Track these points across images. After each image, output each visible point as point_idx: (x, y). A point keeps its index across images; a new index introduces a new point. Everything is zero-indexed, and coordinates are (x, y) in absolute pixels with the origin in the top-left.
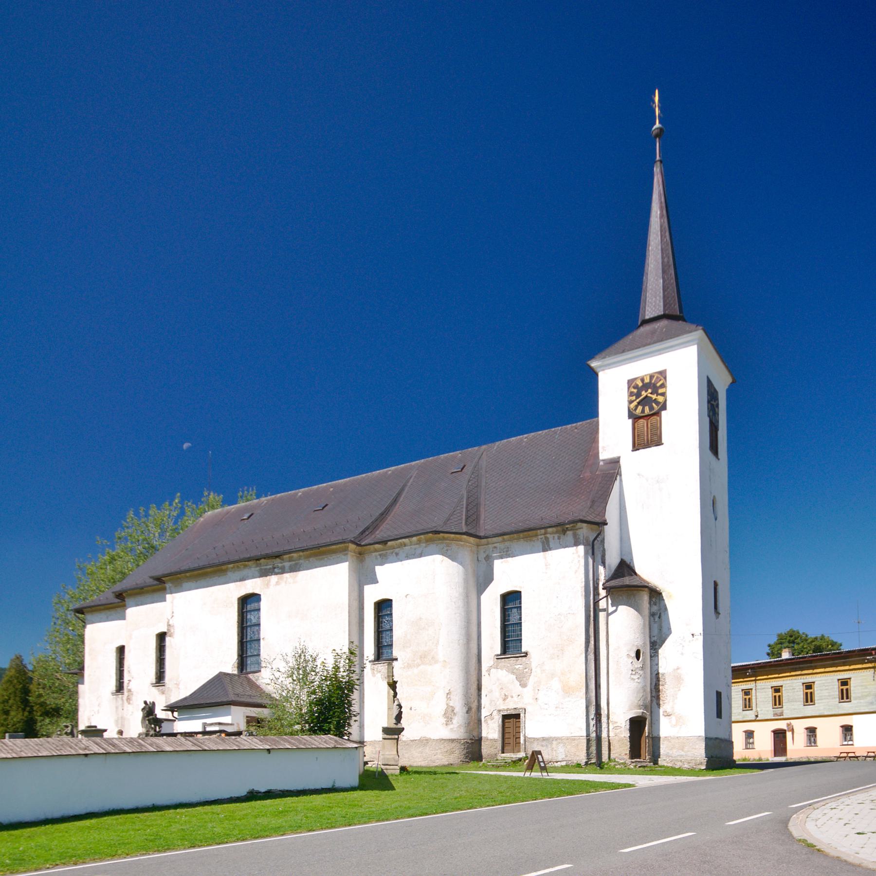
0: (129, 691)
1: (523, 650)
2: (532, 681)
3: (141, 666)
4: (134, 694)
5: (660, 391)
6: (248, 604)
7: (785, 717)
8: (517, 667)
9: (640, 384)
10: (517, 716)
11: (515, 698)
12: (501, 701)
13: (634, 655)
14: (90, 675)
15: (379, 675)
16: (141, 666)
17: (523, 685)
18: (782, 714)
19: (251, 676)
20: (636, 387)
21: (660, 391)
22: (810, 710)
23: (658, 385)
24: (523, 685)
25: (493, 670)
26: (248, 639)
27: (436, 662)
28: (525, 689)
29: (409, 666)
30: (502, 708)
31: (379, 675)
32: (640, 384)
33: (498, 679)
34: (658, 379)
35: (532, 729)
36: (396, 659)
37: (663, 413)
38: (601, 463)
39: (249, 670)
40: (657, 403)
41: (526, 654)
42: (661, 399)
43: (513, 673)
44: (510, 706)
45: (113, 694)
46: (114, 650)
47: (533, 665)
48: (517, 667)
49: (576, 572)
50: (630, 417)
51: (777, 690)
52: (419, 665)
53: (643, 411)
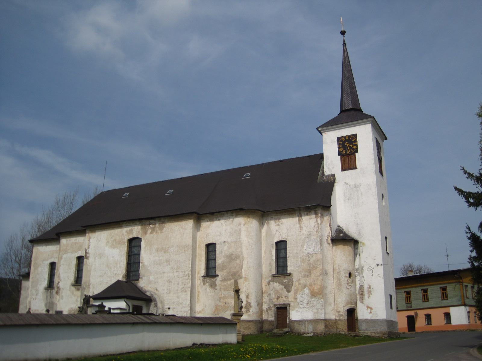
0: (58, 288)
1: (288, 272)
2: (293, 289)
3: (66, 275)
4: (61, 289)
5: (354, 144)
6: (134, 244)
7: (413, 308)
8: (285, 281)
9: (344, 140)
10: (286, 308)
11: (284, 299)
12: (276, 299)
13: (348, 275)
14: (33, 278)
15: (207, 284)
16: (66, 275)
17: (289, 291)
18: (411, 307)
19: (133, 282)
20: (342, 141)
21: (354, 144)
22: (426, 305)
23: (353, 141)
24: (289, 291)
25: (271, 283)
26: (132, 261)
28: (290, 294)
29: (225, 280)
30: (276, 303)
31: (207, 284)
32: (344, 140)
33: (274, 288)
34: (353, 138)
35: (294, 315)
37: (356, 154)
39: (131, 279)
40: (353, 149)
41: (290, 275)
42: (355, 147)
43: (283, 284)
44: (281, 302)
46: (49, 264)
47: (294, 280)
48: (285, 281)
49: (317, 232)
50: (339, 155)
51: (408, 293)
53: (346, 152)
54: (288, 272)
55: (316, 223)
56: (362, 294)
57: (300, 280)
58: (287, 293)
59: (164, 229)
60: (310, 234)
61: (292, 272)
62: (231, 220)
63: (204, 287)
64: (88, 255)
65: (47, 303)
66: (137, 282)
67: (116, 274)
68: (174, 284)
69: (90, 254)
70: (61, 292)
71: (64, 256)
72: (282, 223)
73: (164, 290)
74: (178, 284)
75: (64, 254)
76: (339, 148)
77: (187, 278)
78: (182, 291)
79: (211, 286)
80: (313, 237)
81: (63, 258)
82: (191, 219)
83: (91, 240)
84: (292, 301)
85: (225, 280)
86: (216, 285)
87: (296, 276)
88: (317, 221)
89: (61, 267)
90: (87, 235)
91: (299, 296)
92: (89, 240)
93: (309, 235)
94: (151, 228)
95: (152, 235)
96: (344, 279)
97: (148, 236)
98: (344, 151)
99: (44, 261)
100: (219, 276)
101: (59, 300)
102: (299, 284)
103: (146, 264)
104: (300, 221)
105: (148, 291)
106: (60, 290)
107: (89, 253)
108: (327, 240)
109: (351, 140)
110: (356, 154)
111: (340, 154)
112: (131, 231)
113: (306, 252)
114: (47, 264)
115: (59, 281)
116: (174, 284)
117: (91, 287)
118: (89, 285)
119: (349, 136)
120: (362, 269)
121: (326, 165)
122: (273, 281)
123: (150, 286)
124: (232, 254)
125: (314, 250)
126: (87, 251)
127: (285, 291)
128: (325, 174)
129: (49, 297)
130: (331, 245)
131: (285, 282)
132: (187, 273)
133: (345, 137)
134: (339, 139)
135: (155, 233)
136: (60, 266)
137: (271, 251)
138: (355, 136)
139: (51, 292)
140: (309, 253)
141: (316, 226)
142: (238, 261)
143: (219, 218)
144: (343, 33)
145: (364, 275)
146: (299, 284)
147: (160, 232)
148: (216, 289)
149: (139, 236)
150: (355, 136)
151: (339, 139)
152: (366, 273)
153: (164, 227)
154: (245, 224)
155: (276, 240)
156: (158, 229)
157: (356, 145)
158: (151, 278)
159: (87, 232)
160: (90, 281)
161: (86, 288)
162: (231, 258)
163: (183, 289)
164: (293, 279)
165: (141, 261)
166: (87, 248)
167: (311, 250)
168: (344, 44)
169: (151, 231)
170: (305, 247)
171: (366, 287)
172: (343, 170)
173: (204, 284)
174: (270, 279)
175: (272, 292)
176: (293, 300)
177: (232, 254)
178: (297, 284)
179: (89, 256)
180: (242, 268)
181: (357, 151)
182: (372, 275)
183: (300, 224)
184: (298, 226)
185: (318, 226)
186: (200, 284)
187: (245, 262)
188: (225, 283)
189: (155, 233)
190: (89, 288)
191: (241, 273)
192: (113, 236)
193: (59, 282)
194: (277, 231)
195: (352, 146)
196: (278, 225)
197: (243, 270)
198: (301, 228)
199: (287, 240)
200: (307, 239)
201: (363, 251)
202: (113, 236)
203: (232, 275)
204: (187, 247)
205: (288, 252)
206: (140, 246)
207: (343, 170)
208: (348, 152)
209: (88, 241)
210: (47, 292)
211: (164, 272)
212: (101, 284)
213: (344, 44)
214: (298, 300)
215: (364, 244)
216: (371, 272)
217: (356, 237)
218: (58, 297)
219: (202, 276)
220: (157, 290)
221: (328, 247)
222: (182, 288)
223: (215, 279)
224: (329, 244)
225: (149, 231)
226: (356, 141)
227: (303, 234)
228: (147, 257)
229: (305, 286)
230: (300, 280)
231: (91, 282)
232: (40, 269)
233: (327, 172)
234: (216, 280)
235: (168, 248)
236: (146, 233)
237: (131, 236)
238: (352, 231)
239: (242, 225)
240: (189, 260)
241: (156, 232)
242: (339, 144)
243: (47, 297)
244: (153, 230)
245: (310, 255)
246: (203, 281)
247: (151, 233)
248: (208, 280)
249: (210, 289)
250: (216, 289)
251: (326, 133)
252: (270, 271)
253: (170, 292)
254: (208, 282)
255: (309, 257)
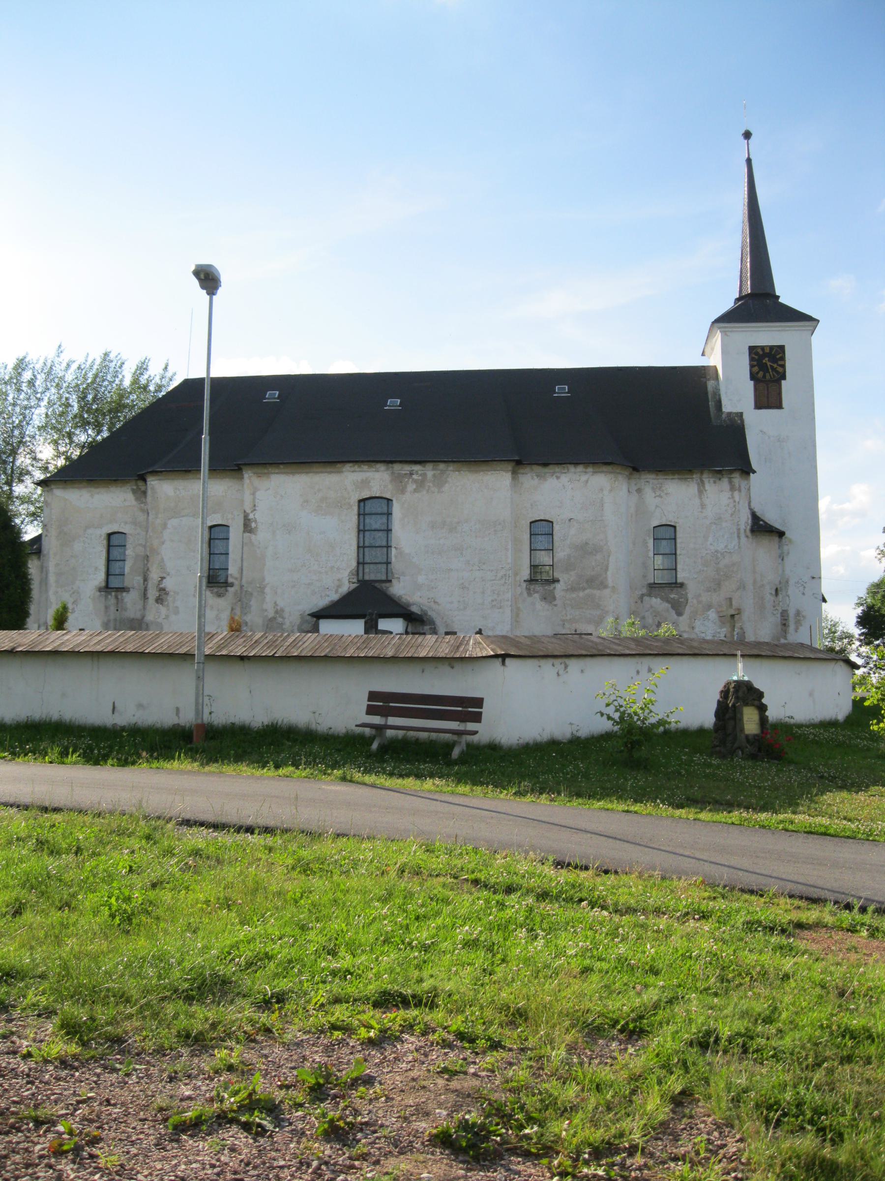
2: (688, 611)
3: (180, 564)
4: (171, 593)
5: (780, 363)
9: (761, 353)
13: (774, 593)
14: (57, 565)
15: (537, 595)
17: (679, 614)
20: (757, 354)
21: (780, 363)
23: (778, 357)
24: (679, 614)
25: (646, 598)
27: (606, 587)
28: (681, 618)
29: (573, 589)
32: (761, 353)
33: (652, 607)
36: (558, 581)
37: (783, 382)
38: (724, 416)
40: (778, 373)
41: (682, 585)
42: (780, 369)
43: (668, 602)
45: (100, 590)
46: (104, 536)
47: (690, 596)
48: (672, 596)
49: (732, 515)
50: (752, 379)
52: (584, 589)
53: (764, 376)
54: (679, 581)
55: (731, 500)
56: (784, 625)
57: (700, 595)
58: (675, 616)
59: (446, 487)
60: (720, 518)
61: (686, 582)
62: (584, 478)
63: (529, 599)
64: (253, 525)
65: (109, 621)
66: (387, 585)
67: (332, 568)
68: (474, 593)
69: (259, 524)
70: (170, 599)
71: (174, 522)
72: (667, 494)
73: (452, 603)
74: (483, 593)
75: (172, 517)
76: (752, 366)
77: (503, 581)
78: (493, 607)
79: (544, 598)
80: (724, 524)
81: (169, 526)
82: (507, 471)
83: (258, 494)
84: (685, 631)
85: (573, 589)
86: (554, 598)
87: (692, 589)
88: (733, 497)
89: (164, 546)
90: (246, 480)
91: (697, 623)
92: (254, 494)
93: (719, 519)
94: (415, 481)
95: (417, 495)
96: (769, 598)
97: (407, 496)
98: (761, 374)
99: (87, 527)
100: (561, 582)
101: (167, 617)
102: (699, 602)
103: (407, 551)
104: (701, 492)
105: (414, 604)
106: (167, 594)
107: (256, 521)
108: (745, 530)
109: (774, 356)
110: (783, 382)
111: (753, 377)
112: (365, 483)
113: (712, 548)
114: (101, 536)
115: (164, 575)
116: (474, 593)
117: (267, 590)
118: (262, 590)
119: (772, 348)
120: (787, 582)
121: (726, 393)
122: (650, 595)
123: (419, 594)
124: (587, 543)
125: (726, 546)
126: (251, 516)
127: (673, 612)
128: (724, 410)
129: (113, 609)
130: (750, 540)
131: (673, 599)
132: (502, 573)
133: (763, 348)
134: (752, 349)
135: (425, 492)
136: (163, 543)
137: (645, 543)
138: (782, 348)
139: (116, 597)
140: (717, 551)
141: (731, 505)
142: (599, 557)
143: (558, 475)
144: (747, 135)
145: (789, 593)
146: (699, 602)
147: (436, 490)
148: (556, 605)
149: (388, 496)
150: (782, 348)
151: (752, 349)
152: (792, 590)
153: (446, 482)
154: (611, 491)
155: (656, 523)
156: (431, 485)
157: (783, 366)
158: (421, 579)
159: (246, 476)
160: (263, 579)
161: (255, 594)
162: (585, 550)
163: (494, 603)
164: (687, 593)
165: (393, 544)
166: (248, 511)
167: (721, 547)
168: (749, 161)
169: (414, 487)
170: (710, 539)
171: (792, 613)
172: (759, 405)
173: (530, 595)
174: (645, 591)
175: (647, 614)
176: (687, 629)
177: (587, 543)
178: (695, 601)
179: (256, 528)
180: (607, 570)
181: (784, 377)
182: (804, 594)
183: (701, 499)
184: (697, 501)
185: (735, 506)
186: (521, 594)
187: (612, 559)
188: (574, 596)
189: (425, 492)
190: (263, 593)
191: (606, 578)
192: (319, 490)
193: (163, 578)
194: (657, 506)
195: (775, 366)
196: (660, 496)
197: (609, 573)
198: (703, 506)
199: (677, 525)
200: (714, 527)
201: (788, 553)
202: (319, 490)
203: (587, 581)
204: (500, 524)
205: (678, 545)
206: (389, 514)
207: (759, 405)
208: (768, 377)
209: (252, 497)
210: (106, 597)
211: (450, 570)
212: (293, 587)
213: (749, 161)
214: (697, 630)
215: (790, 541)
216: (801, 588)
217: (777, 525)
218: (163, 610)
219: (526, 578)
220: (435, 602)
221: (747, 543)
222: (493, 601)
223: (553, 586)
224: (747, 537)
225: (411, 487)
226: (783, 358)
227: (706, 517)
228: (407, 536)
229: (709, 607)
230: (700, 595)
231: (266, 582)
232: (78, 546)
233: (728, 407)
234: (555, 588)
235: (458, 523)
236: (403, 491)
237: (366, 494)
238: (771, 517)
239: (606, 492)
240: (507, 549)
241: (428, 491)
242: (752, 359)
243: (107, 608)
244: (421, 484)
245: (719, 555)
246: (528, 589)
247: (415, 491)
248: (538, 587)
249: (543, 603)
250: (556, 605)
251: (728, 334)
252: (644, 576)
253: (465, 608)
254: (537, 592)
255: (717, 558)
